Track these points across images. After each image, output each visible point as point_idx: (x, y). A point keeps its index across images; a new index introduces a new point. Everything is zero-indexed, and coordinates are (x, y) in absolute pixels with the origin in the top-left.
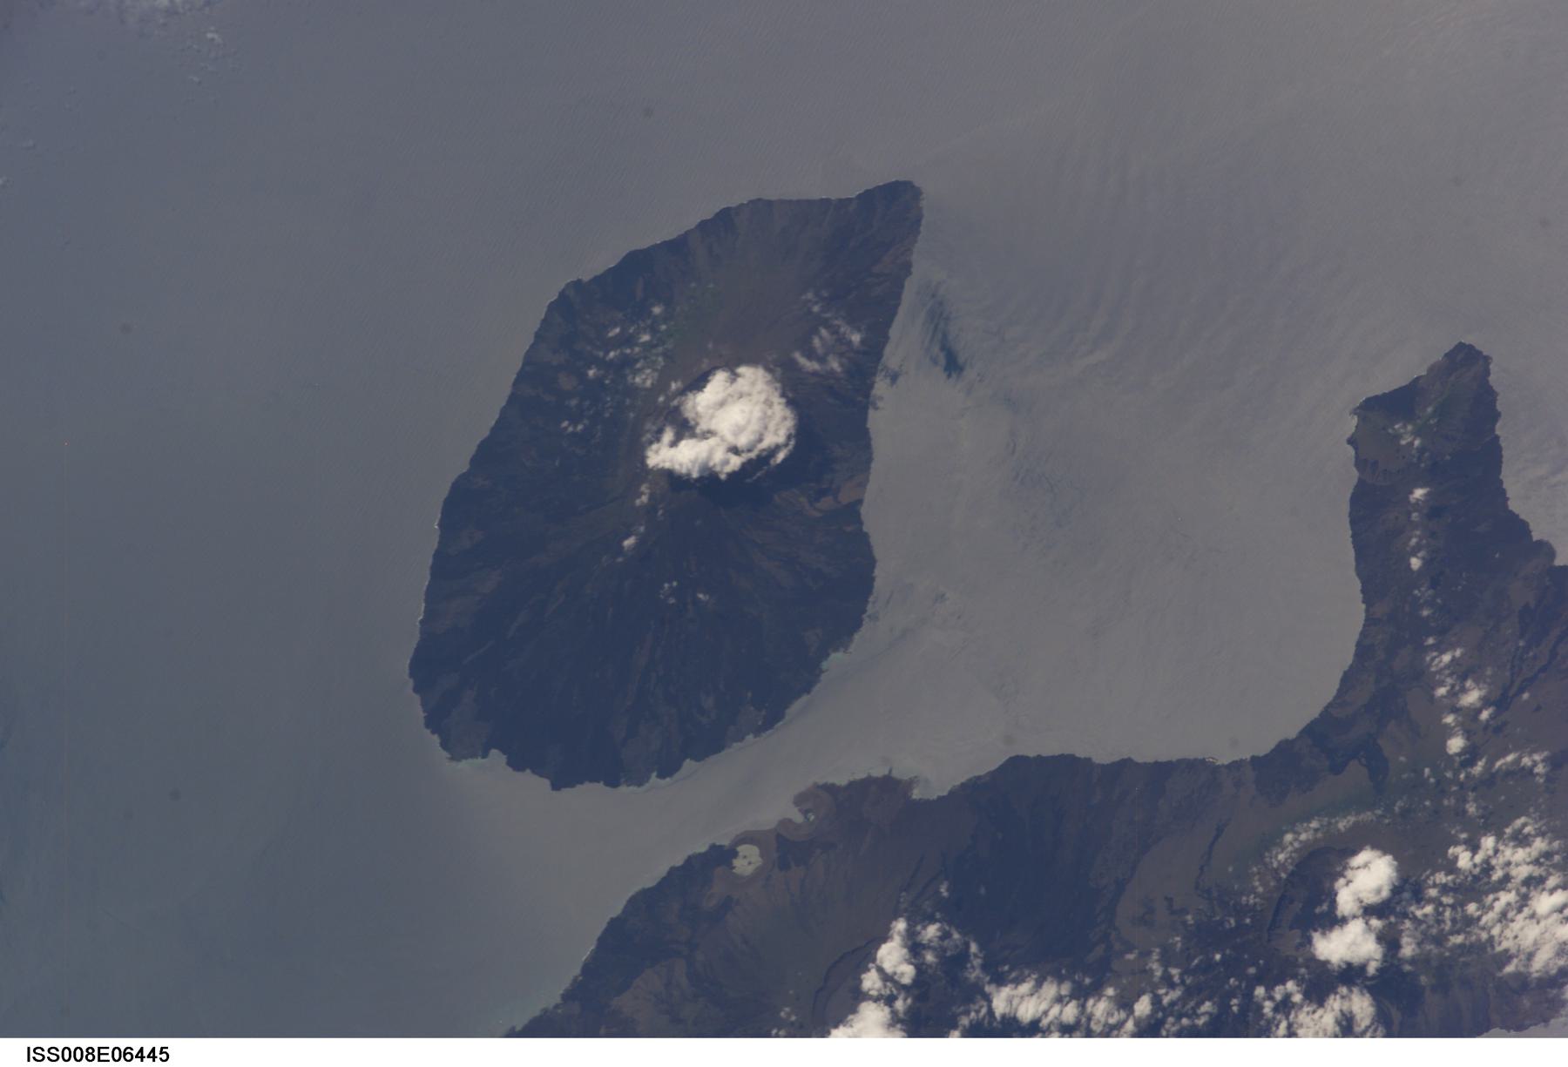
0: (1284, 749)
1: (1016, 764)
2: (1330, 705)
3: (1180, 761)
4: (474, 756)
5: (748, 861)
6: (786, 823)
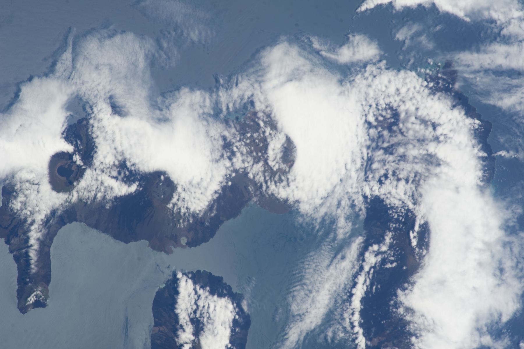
0: (70, 222)
1: (127, 242)
2: (60, 229)
3: (92, 227)
4: (239, 294)
5: (184, 241)
6: (175, 247)
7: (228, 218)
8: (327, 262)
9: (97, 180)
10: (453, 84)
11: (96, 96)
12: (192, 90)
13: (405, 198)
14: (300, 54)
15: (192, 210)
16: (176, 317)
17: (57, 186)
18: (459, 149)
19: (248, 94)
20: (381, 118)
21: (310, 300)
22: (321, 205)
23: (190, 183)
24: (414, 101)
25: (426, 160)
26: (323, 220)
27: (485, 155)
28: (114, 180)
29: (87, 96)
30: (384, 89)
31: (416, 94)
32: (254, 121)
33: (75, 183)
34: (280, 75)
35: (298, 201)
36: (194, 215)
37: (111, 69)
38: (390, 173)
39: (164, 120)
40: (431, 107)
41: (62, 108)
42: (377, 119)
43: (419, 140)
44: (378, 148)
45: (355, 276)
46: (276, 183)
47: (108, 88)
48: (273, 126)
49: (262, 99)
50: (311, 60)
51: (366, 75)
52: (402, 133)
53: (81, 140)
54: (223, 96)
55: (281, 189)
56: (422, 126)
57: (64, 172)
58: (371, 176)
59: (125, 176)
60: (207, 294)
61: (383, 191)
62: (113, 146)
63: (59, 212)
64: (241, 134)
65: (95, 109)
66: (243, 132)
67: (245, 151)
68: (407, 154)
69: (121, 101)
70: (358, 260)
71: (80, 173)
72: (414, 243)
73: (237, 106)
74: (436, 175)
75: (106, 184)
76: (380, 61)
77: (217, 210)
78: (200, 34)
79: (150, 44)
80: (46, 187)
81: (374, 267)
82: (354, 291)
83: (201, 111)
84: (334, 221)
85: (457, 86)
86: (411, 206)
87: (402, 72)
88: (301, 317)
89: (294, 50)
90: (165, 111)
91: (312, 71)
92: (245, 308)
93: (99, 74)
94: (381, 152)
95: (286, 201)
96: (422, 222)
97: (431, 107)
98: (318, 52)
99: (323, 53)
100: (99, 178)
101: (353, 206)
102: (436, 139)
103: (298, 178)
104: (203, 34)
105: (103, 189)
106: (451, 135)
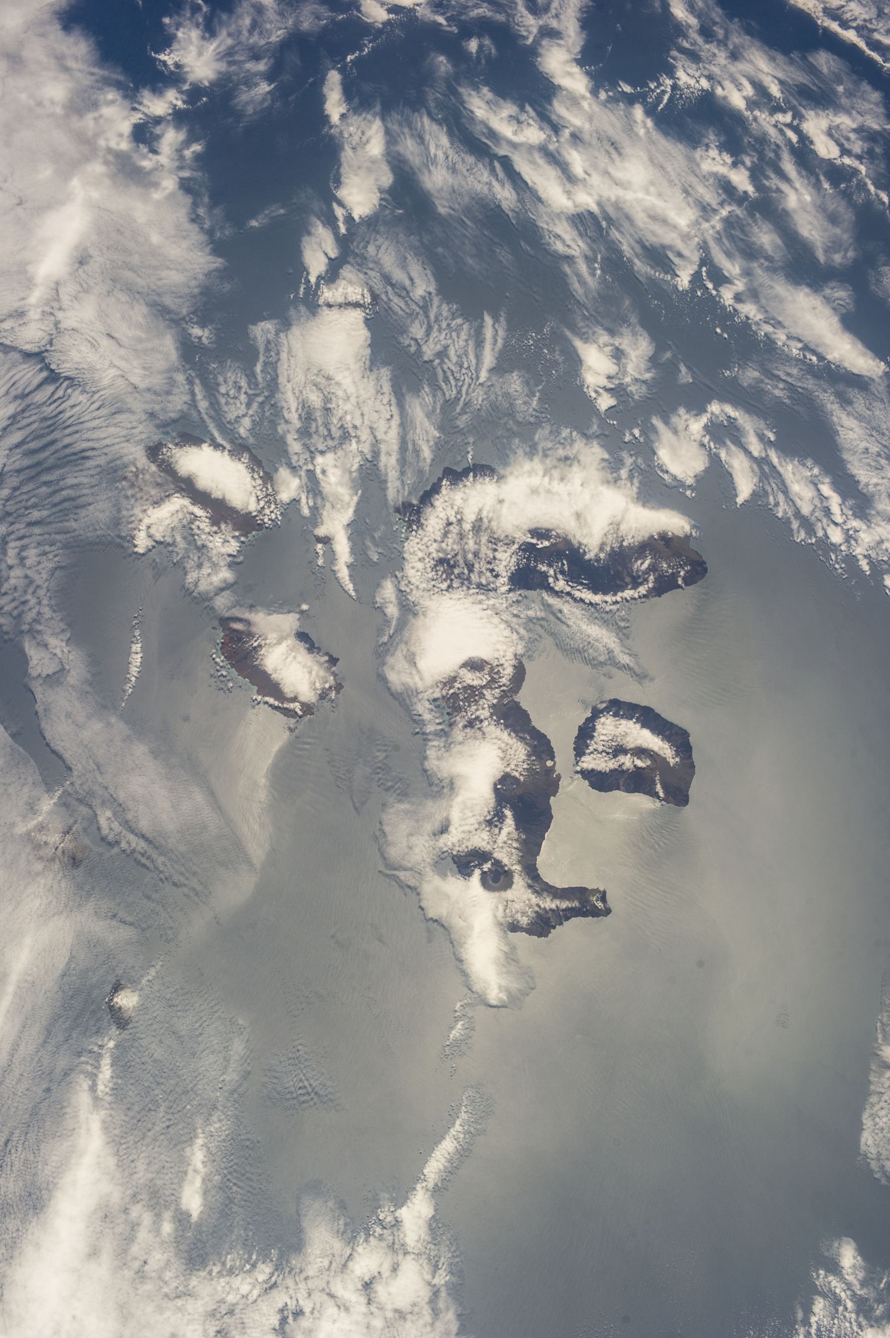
1: (552, 817)
5: (549, 763)
7: (530, 720)
8: (564, 627)
9: (502, 847)
10: (414, 506)
11: (434, 849)
12: (425, 758)
13: (510, 552)
14: (392, 655)
15: (525, 758)
16: (611, 771)
17: (508, 885)
18: (467, 500)
20: (444, 576)
21: (596, 644)
22: (518, 633)
23: (502, 759)
24: (429, 544)
25: (478, 531)
26: (529, 630)
27: (471, 474)
28: (502, 831)
29: (434, 857)
30: (419, 573)
31: (423, 542)
32: (448, 699)
33: (506, 869)
34: (411, 674)
35: (515, 655)
36: (529, 756)
37: (411, 835)
38: (489, 566)
39: (452, 785)
40: (433, 527)
41: (444, 880)
42: (445, 580)
43: (461, 539)
44: (469, 579)
45: (575, 600)
46: (500, 678)
47: (427, 837)
48: (453, 680)
49: (431, 691)
50: (397, 644)
51: (408, 590)
52: (456, 555)
53: (470, 862)
54: (430, 728)
55: (506, 672)
56: (450, 536)
57: (497, 879)
58: (492, 586)
59: (498, 821)
60: (593, 742)
61: (504, 574)
62: (474, 832)
63: (529, 881)
64: (461, 711)
65: (445, 849)
66: (458, 709)
67: (474, 707)
68: (473, 550)
69: (437, 825)
70: (562, 597)
71: (497, 863)
72: (546, 543)
73: (437, 715)
74: (489, 522)
75: (506, 839)
76: (396, 576)
77: (524, 732)
78: (379, 750)
80: (509, 894)
81: (567, 581)
82: (587, 601)
83: (443, 749)
84: (530, 620)
85: (415, 502)
86: (516, 546)
87: (405, 556)
88: (610, 652)
89: (390, 660)
90: (443, 784)
91: (406, 643)
92: (604, 705)
93: (416, 846)
94: (472, 575)
96: (529, 536)
97: (433, 527)
98: (391, 637)
99: (391, 632)
100: (501, 845)
101: (518, 602)
102: (460, 522)
103: (496, 656)
104: (379, 747)
105: (510, 842)
106: (456, 508)
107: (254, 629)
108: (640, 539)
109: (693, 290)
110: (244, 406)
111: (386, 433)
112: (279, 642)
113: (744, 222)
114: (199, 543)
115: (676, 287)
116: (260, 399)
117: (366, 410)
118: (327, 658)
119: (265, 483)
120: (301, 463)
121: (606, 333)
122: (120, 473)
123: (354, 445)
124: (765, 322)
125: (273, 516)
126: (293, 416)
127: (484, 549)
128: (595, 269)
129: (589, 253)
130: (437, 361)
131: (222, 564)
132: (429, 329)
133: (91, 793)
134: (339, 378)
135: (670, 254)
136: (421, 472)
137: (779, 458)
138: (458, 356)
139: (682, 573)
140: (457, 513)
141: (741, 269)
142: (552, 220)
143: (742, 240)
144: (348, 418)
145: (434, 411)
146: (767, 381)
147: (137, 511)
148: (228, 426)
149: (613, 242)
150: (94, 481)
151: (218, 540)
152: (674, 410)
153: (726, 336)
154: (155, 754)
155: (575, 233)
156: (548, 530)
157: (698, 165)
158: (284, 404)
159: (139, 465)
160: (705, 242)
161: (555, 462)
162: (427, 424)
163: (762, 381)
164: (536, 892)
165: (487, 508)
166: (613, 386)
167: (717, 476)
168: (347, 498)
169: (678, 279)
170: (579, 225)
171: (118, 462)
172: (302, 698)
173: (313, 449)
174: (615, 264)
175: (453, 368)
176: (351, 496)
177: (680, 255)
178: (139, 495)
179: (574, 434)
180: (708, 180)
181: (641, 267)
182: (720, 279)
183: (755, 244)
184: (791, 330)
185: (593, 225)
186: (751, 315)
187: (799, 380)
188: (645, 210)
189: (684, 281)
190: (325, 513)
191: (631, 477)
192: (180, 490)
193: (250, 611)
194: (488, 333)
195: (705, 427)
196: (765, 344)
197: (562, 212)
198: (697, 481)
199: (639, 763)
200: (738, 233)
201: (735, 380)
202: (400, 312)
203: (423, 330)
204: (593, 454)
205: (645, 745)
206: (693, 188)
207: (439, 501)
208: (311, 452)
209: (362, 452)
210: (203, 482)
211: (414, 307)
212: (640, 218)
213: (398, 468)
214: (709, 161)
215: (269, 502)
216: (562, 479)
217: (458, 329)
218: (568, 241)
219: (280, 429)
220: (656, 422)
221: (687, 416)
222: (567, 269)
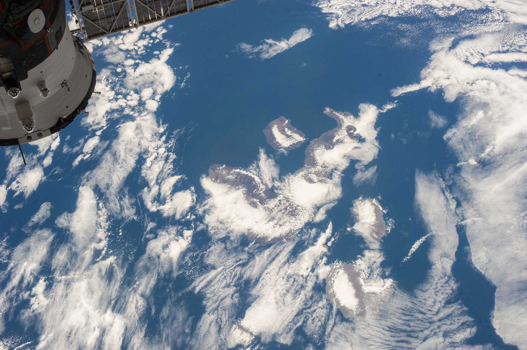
8: (273, 175)
13: (269, 206)
19: (334, 179)
26: (284, 180)
39: (345, 156)
44: (289, 205)
48: (320, 181)
54: (339, 173)
68: (280, 213)
71: (347, 131)
72: (255, 200)
79: (366, 163)
80: (351, 124)
85: (285, 240)
86: (265, 206)
88: (266, 161)
95: (298, 173)
98: (329, 203)
101: (280, 190)
102: (276, 224)
106: (274, 229)
107: (371, 231)
108: (224, 185)
109: (111, 255)
110: (317, 312)
111: (274, 269)
112: (366, 223)
113: (61, 268)
114: (369, 270)
115: (116, 260)
116: (308, 310)
117: (274, 282)
118: (354, 209)
119: (332, 277)
120: (313, 277)
121: (161, 257)
122: (380, 313)
123: (290, 271)
124: (100, 226)
125: (337, 263)
126: (302, 297)
127: (276, 212)
128: (137, 285)
129: (133, 292)
130: (231, 284)
131: (366, 259)
132: (222, 300)
133: (453, 215)
134: (274, 301)
135: (103, 273)
136: (275, 248)
137: (151, 182)
138: (222, 281)
139: (221, 168)
140: (275, 227)
141: (85, 251)
142: (131, 316)
143: (70, 262)
144: (282, 283)
145: (250, 267)
146: (125, 207)
147: (383, 295)
148: (328, 307)
149: (119, 292)
150: (391, 316)
151: (362, 267)
152: (169, 217)
153: (120, 231)
154: (427, 214)
155: (128, 305)
156: (250, 204)
157: (48, 305)
158: (301, 303)
159: (372, 312)
160: (85, 270)
161: (226, 224)
162: (257, 263)
163: (128, 208)
164: (343, 122)
165: (263, 223)
166: (180, 237)
167: (177, 188)
168: (307, 255)
169: (112, 261)
170: (123, 307)
171: (379, 318)
172: (370, 203)
173: (305, 279)
174: (129, 281)
175: (228, 278)
176: (305, 255)
177: (100, 271)
178: (379, 300)
179: (210, 229)
180: (52, 295)
181: (119, 275)
182: (97, 253)
183: (68, 258)
184: (96, 219)
185: (118, 306)
186: (103, 232)
187: (114, 201)
188: (92, 298)
189: (111, 259)
190: (319, 254)
191: (206, 204)
192: (363, 292)
193: (368, 238)
194: (202, 284)
195: (163, 205)
196: (110, 220)
197: (124, 317)
198: (186, 190)
199: (286, 129)
200: (69, 266)
201: (137, 213)
202: (227, 313)
203: (225, 300)
204: (210, 220)
205: (280, 133)
206: (62, 295)
207: (277, 235)
208: (306, 279)
209: (289, 268)
210: (353, 291)
211: (220, 312)
212: (97, 296)
213: (281, 254)
214: (41, 304)
215: (335, 269)
216: (229, 217)
217: (213, 292)
218: (135, 303)
219: (310, 294)
220: (178, 217)
221: (166, 211)
222: (148, 292)
